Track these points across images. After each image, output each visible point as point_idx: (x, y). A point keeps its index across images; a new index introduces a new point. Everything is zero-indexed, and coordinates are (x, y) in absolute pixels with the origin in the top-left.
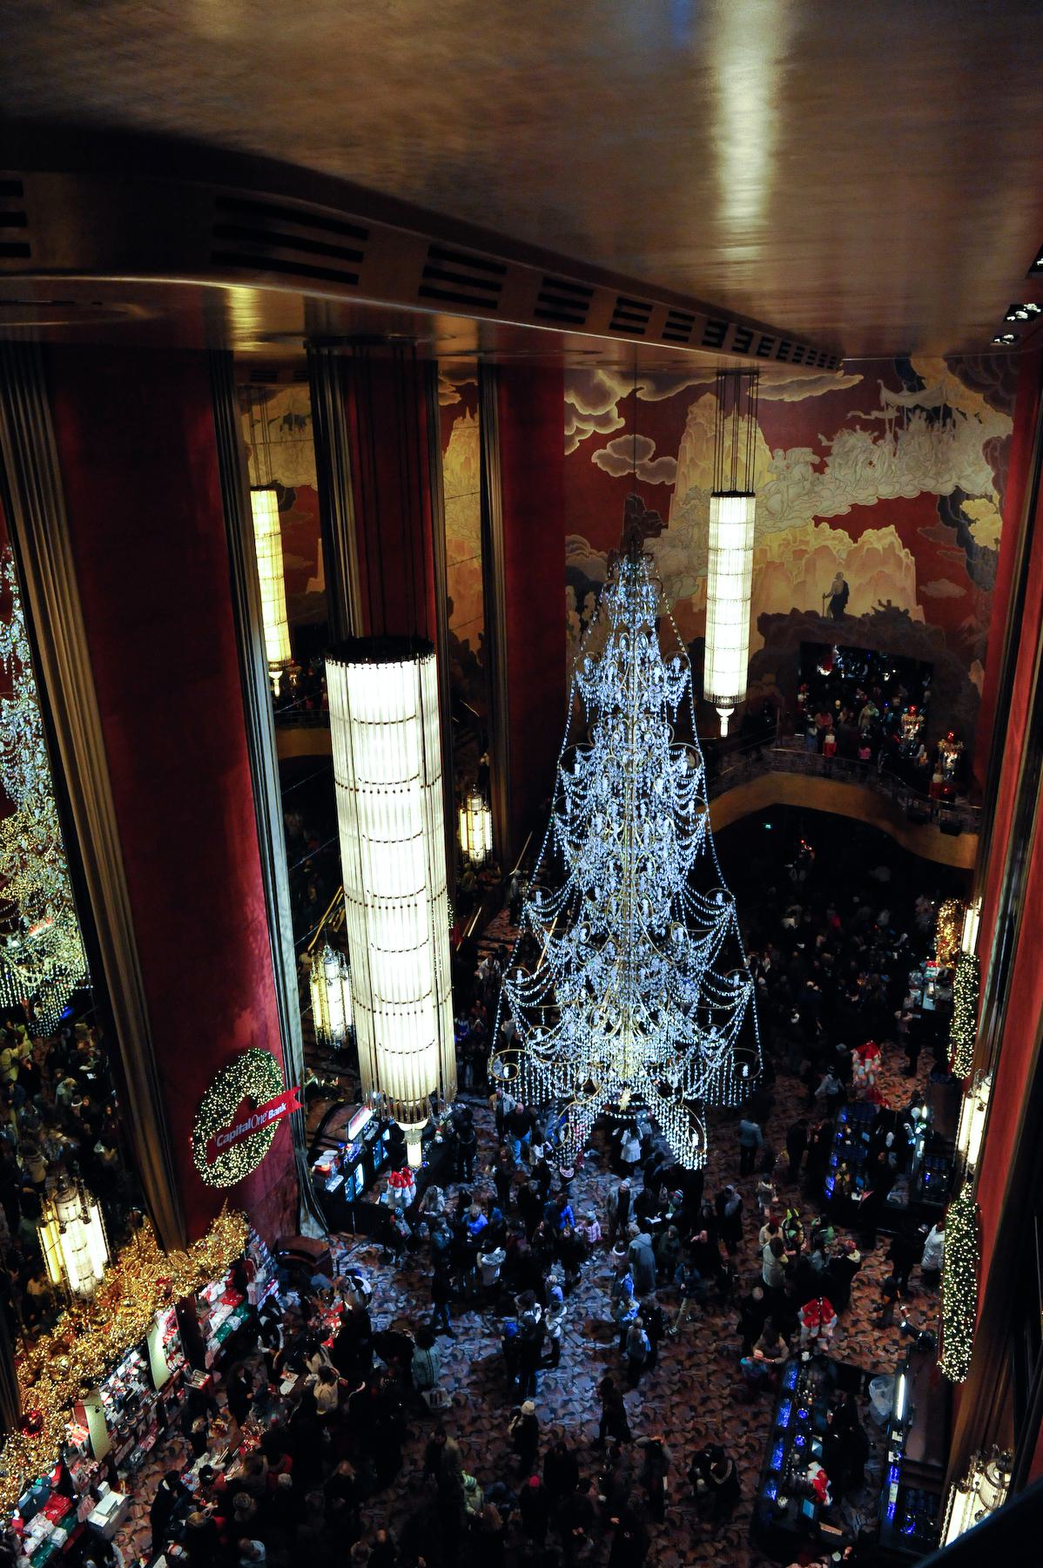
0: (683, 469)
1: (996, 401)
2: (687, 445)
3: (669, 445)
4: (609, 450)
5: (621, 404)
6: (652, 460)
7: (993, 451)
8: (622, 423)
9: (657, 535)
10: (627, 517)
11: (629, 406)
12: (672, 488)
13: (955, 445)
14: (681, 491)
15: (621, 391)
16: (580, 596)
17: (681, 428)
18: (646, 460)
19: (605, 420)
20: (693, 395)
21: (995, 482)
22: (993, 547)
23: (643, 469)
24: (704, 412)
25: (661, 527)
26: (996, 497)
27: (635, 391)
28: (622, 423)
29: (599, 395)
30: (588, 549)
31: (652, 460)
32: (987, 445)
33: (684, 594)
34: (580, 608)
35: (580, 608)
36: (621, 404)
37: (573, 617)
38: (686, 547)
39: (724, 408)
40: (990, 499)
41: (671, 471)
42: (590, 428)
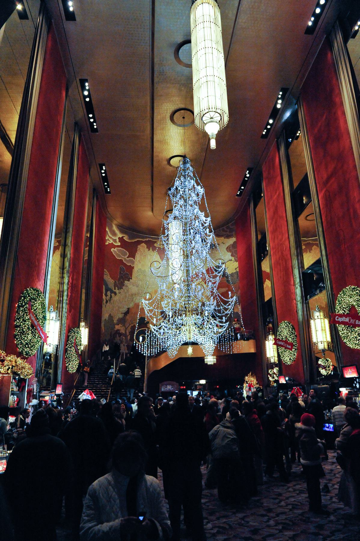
0: (136, 263)
1: (228, 237)
2: (138, 256)
3: (132, 255)
4: (116, 250)
5: (119, 238)
6: (128, 257)
7: (228, 249)
8: (119, 244)
9: (129, 281)
10: (120, 272)
11: (121, 239)
12: (133, 268)
13: (217, 252)
14: (135, 269)
15: (120, 235)
16: (107, 291)
17: (136, 251)
18: (126, 257)
19: (115, 241)
20: (139, 243)
21: (232, 255)
22: (235, 271)
23: (125, 259)
24: (142, 247)
25: (130, 279)
26: (233, 258)
27: (123, 237)
28: (119, 244)
29: (114, 234)
30: (109, 277)
31: (128, 257)
32: (227, 248)
33: (137, 301)
34: (106, 295)
35: (106, 295)
36: (119, 238)
37: (104, 297)
38: (138, 287)
39: (148, 248)
40: (231, 260)
41: (133, 262)
42: (111, 241)
